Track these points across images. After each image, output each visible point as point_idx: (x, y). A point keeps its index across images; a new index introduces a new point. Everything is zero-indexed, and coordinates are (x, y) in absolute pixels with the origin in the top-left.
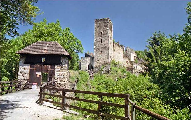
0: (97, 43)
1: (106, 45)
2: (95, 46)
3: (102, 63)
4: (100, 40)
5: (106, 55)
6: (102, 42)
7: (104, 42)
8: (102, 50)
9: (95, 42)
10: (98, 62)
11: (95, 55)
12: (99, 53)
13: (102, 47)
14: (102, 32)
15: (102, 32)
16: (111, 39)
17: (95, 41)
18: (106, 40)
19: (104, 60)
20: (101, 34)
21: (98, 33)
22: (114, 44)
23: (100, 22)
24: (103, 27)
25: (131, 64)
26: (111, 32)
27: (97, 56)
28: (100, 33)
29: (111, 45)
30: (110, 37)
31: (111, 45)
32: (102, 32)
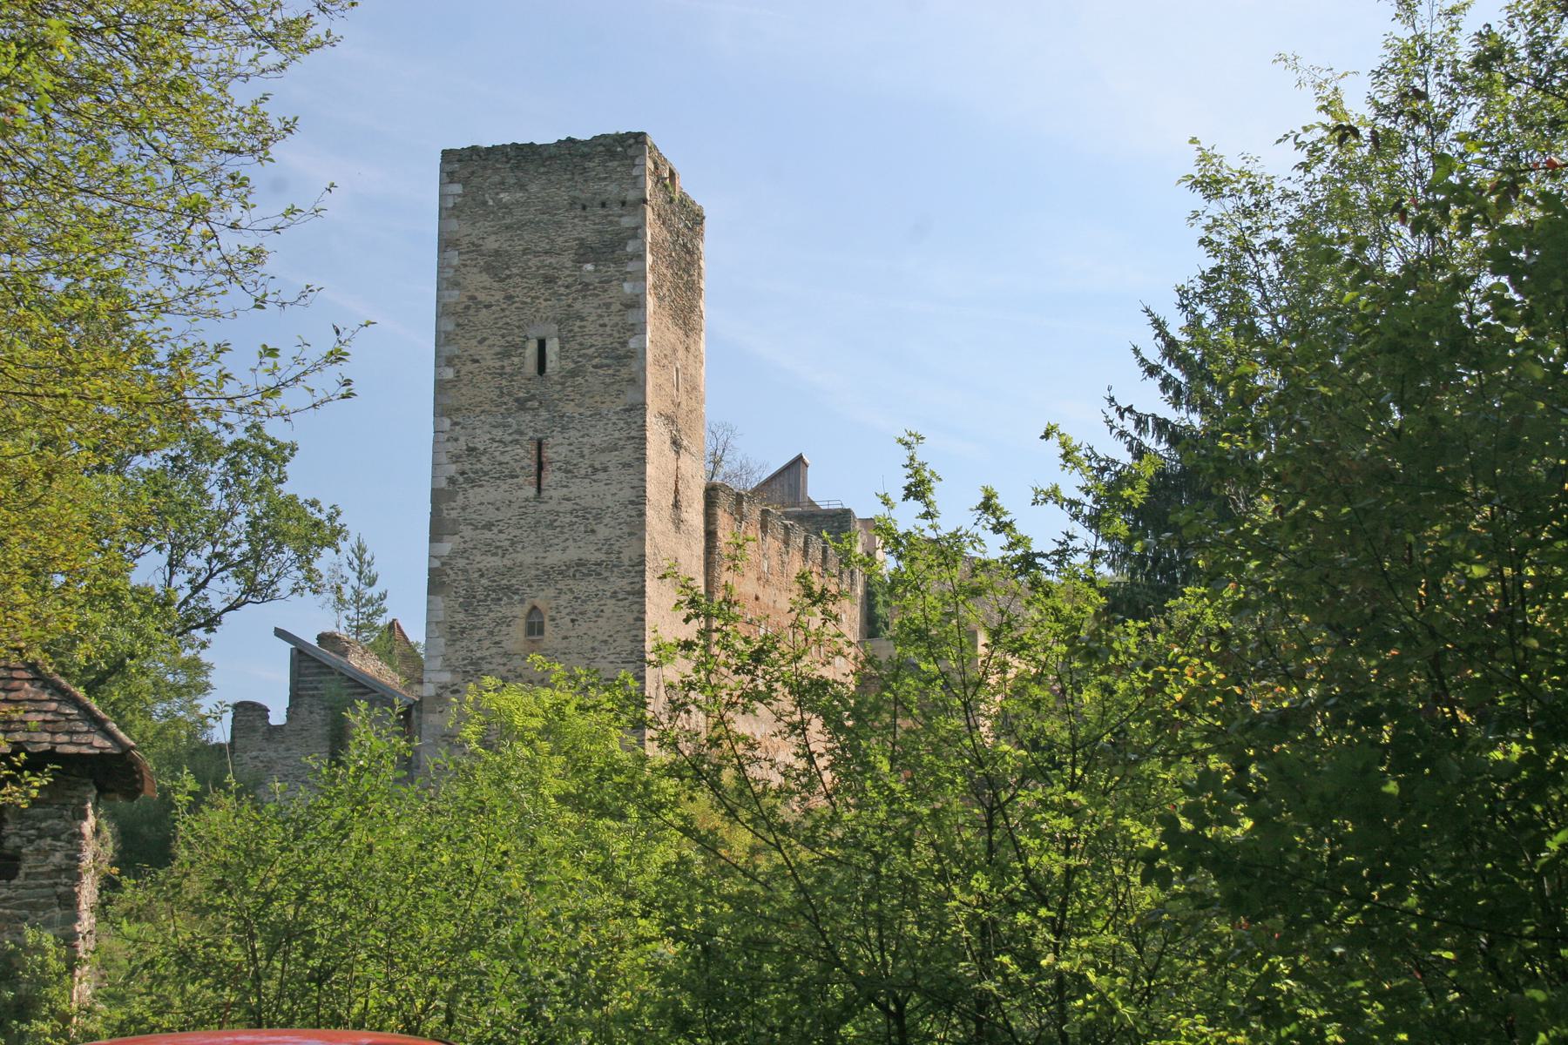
0: (475, 495)
1: (603, 532)
6: (550, 478)
7: (579, 488)
8: (542, 598)
11: (446, 677)
13: (555, 558)
14: (542, 344)
15: (553, 347)
16: (675, 443)
18: (612, 459)
22: (723, 519)
23: (522, 187)
24: (567, 260)
26: (673, 335)
29: (678, 522)
30: (670, 420)
31: (678, 522)
32: (542, 344)
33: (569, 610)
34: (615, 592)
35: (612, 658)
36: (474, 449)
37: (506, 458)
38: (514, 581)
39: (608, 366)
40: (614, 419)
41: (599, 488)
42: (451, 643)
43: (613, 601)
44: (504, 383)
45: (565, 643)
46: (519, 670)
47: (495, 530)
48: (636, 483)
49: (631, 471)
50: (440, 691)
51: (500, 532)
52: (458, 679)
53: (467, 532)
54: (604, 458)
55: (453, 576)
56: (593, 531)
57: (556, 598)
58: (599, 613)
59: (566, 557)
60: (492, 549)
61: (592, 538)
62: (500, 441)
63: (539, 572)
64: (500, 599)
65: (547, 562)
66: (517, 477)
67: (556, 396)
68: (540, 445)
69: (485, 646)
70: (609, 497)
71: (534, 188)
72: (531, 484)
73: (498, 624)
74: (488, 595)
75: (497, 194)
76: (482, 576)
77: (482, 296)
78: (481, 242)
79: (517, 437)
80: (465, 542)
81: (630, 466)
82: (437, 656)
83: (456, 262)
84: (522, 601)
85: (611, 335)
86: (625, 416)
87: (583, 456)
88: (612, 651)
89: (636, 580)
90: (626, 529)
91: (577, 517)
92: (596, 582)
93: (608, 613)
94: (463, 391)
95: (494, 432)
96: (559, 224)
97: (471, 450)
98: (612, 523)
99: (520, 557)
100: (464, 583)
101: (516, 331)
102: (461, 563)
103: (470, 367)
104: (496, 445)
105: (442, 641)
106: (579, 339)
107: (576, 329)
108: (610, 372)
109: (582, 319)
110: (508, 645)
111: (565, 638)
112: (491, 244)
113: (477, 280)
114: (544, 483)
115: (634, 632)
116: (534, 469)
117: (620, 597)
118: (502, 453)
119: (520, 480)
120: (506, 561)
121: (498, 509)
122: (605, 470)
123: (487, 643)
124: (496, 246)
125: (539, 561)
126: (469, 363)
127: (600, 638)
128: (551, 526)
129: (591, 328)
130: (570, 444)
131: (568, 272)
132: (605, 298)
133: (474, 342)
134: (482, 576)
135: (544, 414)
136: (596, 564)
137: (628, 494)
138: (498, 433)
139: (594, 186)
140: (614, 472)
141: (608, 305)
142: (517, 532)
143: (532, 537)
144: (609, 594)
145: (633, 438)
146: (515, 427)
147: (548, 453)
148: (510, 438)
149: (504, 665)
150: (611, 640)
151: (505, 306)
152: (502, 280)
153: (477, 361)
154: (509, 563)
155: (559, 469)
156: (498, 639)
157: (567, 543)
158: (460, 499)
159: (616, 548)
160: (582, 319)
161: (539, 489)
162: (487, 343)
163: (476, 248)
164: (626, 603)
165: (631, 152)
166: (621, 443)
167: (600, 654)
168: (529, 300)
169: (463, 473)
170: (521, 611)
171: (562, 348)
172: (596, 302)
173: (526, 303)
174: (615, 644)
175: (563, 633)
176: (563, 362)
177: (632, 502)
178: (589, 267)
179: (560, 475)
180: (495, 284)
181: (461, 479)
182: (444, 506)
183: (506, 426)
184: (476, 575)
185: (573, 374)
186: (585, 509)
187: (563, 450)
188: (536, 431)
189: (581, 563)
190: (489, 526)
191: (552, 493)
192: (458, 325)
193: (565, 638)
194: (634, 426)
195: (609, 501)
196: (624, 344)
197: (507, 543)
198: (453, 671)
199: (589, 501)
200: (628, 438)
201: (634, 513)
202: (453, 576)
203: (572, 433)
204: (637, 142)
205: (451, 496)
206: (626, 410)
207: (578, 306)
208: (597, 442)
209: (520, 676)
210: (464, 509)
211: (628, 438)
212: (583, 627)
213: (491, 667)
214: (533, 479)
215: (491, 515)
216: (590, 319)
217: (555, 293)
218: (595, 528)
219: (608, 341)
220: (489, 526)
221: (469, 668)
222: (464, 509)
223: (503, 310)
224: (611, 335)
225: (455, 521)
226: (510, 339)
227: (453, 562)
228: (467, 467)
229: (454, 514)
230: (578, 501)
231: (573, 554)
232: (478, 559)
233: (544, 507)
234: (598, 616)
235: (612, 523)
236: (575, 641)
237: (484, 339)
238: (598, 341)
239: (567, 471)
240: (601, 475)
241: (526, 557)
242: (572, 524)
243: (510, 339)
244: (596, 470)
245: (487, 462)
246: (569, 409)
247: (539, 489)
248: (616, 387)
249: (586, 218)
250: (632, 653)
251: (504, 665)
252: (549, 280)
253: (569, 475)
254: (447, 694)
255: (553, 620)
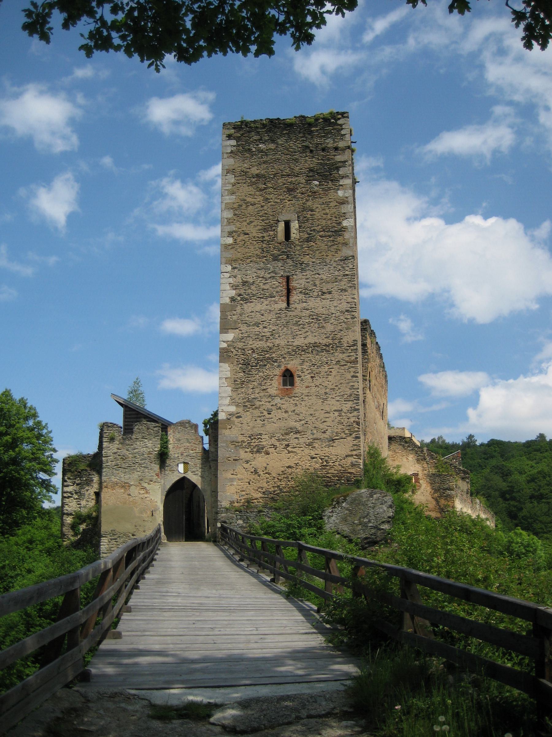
0: (248, 307)
1: (329, 327)
2: (230, 336)
3: (299, 471)
4: (278, 285)
5: (333, 404)
6: (295, 297)
7: (314, 303)
8: (293, 364)
9: (233, 299)
10: (260, 461)
11: (233, 409)
12: (273, 391)
13: (299, 341)
14: (287, 224)
15: (295, 225)
17: (233, 293)
19: (321, 450)
20: (281, 236)
21: (254, 231)
23: (273, 141)
24: (302, 179)
25: (436, 491)
27: (247, 417)
28: (271, 227)
32: (287, 224)
33: (310, 371)
34: (339, 361)
35: (338, 398)
36: (246, 282)
37: (266, 287)
38: (274, 355)
39: (330, 236)
40: (334, 265)
41: (326, 303)
42: (235, 390)
43: (338, 366)
44: (264, 245)
45: (307, 390)
46: (279, 405)
47: (261, 327)
48: (350, 300)
49: (346, 293)
50: (229, 417)
51: (265, 327)
52: (240, 410)
53: (244, 328)
54: (329, 286)
55: (235, 352)
56: (323, 327)
57: (301, 364)
58: (329, 373)
59: (306, 341)
60: (259, 337)
61: (323, 331)
62: (262, 277)
63: (290, 350)
64: (265, 365)
65: (295, 344)
66: (274, 297)
67: (297, 253)
68: (288, 278)
69: (257, 392)
70: (333, 308)
71: (280, 142)
72: (282, 301)
73: (264, 379)
74: (258, 363)
75: (257, 145)
76: (254, 352)
77: (249, 199)
78: (248, 170)
79: (274, 275)
80: (242, 333)
81: (345, 290)
82: (226, 397)
83: (233, 181)
84: (279, 366)
85: (331, 219)
86: (341, 263)
87: (316, 286)
88: (338, 394)
89: (352, 354)
90: (344, 325)
91: (313, 319)
92: (327, 355)
93: (334, 373)
94: (239, 250)
95: (259, 272)
96: (296, 160)
97: (244, 283)
98: (335, 323)
99: (277, 342)
100: (242, 356)
101: (271, 217)
102: (240, 345)
103: (242, 237)
104: (261, 279)
105: (229, 389)
106: (311, 221)
107: (309, 216)
108: (331, 239)
109: (312, 210)
110: (273, 391)
111: (307, 387)
112: (255, 171)
113: (246, 190)
114: (291, 302)
115: (352, 384)
116: (285, 292)
117: (342, 364)
118: (264, 284)
119: (277, 298)
120: (268, 344)
121: (262, 315)
122: (330, 293)
123: (257, 391)
124: (258, 172)
125: (290, 343)
126: (242, 235)
127: (330, 387)
128: (297, 324)
129: (317, 215)
130: (307, 279)
131: (303, 186)
132: (325, 199)
133: (245, 224)
134: (254, 352)
135: (289, 261)
136: (326, 345)
137: (344, 306)
138: (262, 273)
139: (317, 140)
140: (335, 294)
141: (327, 203)
142: (274, 328)
143: (284, 331)
144: (334, 362)
145: (347, 275)
146: (272, 269)
147: (293, 284)
148: (269, 276)
149: (269, 402)
150: (337, 388)
151: (264, 204)
152: (261, 190)
153: (248, 234)
154: (271, 345)
155: (301, 292)
156: (265, 387)
157: (308, 334)
158: (239, 309)
159: (338, 336)
160: (312, 210)
161: (288, 304)
162: (253, 224)
163: (244, 173)
164: (346, 367)
165: (340, 122)
166: (340, 278)
167: (330, 396)
168: (279, 201)
169: (240, 295)
170: (278, 372)
171: (300, 227)
172: (321, 200)
173: (276, 202)
174: (340, 391)
175: (306, 384)
176: (301, 234)
177: (347, 311)
178: (317, 183)
179: (301, 296)
180: (257, 193)
181: (239, 298)
182: (228, 313)
183: (266, 269)
184: (250, 352)
185: (308, 240)
186: (317, 315)
187: (303, 282)
188: (285, 272)
189: (315, 345)
190: (257, 324)
191: (296, 305)
192: (235, 215)
193: (307, 387)
194: (347, 268)
195: (333, 310)
196: (340, 223)
197: (269, 334)
198: (237, 406)
199: (320, 310)
200: (344, 275)
201: (349, 317)
202: (235, 352)
203: (308, 272)
204: (344, 117)
205: (233, 309)
206: (341, 260)
207: (309, 203)
208: (325, 277)
209: (280, 408)
210: (241, 315)
211: (344, 275)
212: (318, 381)
213: (261, 403)
214: (284, 298)
215: (258, 318)
216: (317, 210)
217: (295, 197)
218: (324, 325)
219: (329, 222)
220: (257, 324)
221: (247, 404)
222: (241, 315)
223: (262, 206)
224: (331, 219)
225: (235, 322)
226: (267, 221)
227: (236, 345)
228: (242, 292)
229: (235, 317)
230: (313, 310)
231: (311, 339)
232: (250, 343)
233: (290, 313)
234: (328, 375)
235: (335, 323)
236: (314, 389)
237: (251, 222)
238: (324, 223)
239: (305, 294)
240: (328, 296)
241: (283, 343)
242: (309, 323)
243: (267, 221)
244: (324, 293)
245: (255, 289)
246: (306, 259)
247: (288, 304)
248: (335, 247)
249: (313, 157)
250: (351, 395)
251: (269, 402)
252: (290, 190)
253: (307, 296)
254: (234, 419)
255: (300, 377)
